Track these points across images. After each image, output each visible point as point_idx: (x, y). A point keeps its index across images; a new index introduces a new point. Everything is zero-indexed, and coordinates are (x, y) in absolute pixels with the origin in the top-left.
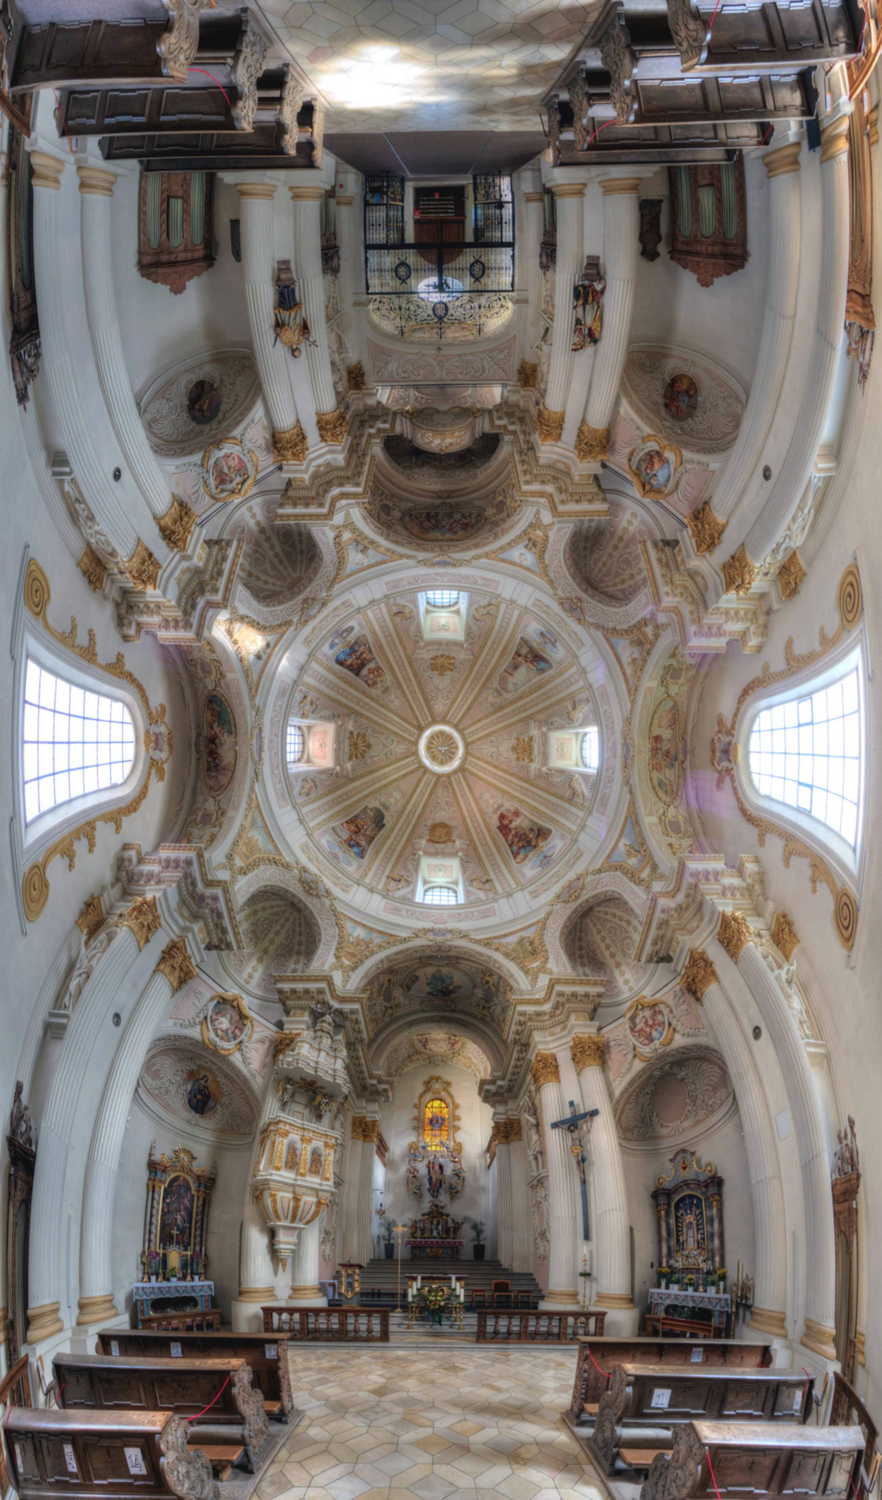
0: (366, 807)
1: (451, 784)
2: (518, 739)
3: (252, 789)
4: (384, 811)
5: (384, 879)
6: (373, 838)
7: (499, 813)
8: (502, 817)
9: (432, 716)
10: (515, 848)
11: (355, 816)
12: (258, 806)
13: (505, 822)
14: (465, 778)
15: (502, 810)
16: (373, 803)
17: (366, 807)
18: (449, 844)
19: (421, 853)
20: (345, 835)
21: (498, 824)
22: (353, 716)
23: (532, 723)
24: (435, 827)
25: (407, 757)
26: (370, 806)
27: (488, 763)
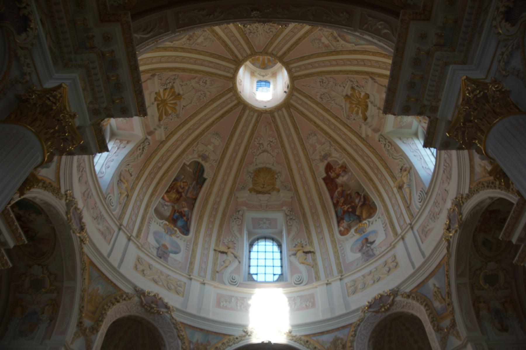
0: (185, 164)
1: (275, 121)
2: (353, 88)
3: (82, 253)
4: (203, 163)
5: (212, 253)
6: (195, 199)
7: (326, 162)
8: (329, 168)
9: (251, 48)
10: (339, 209)
11: (175, 180)
12: (92, 263)
13: (332, 175)
14: (291, 117)
15: (329, 159)
16: (190, 158)
17: (185, 164)
18: (275, 193)
19: (245, 208)
20: (167, 211)
21: (324, 175)
22: (156, 78)
23: (370, 81)
24: (259, 172)
25: (223, 95)
26: (188, 163)
27: (317, 104)
